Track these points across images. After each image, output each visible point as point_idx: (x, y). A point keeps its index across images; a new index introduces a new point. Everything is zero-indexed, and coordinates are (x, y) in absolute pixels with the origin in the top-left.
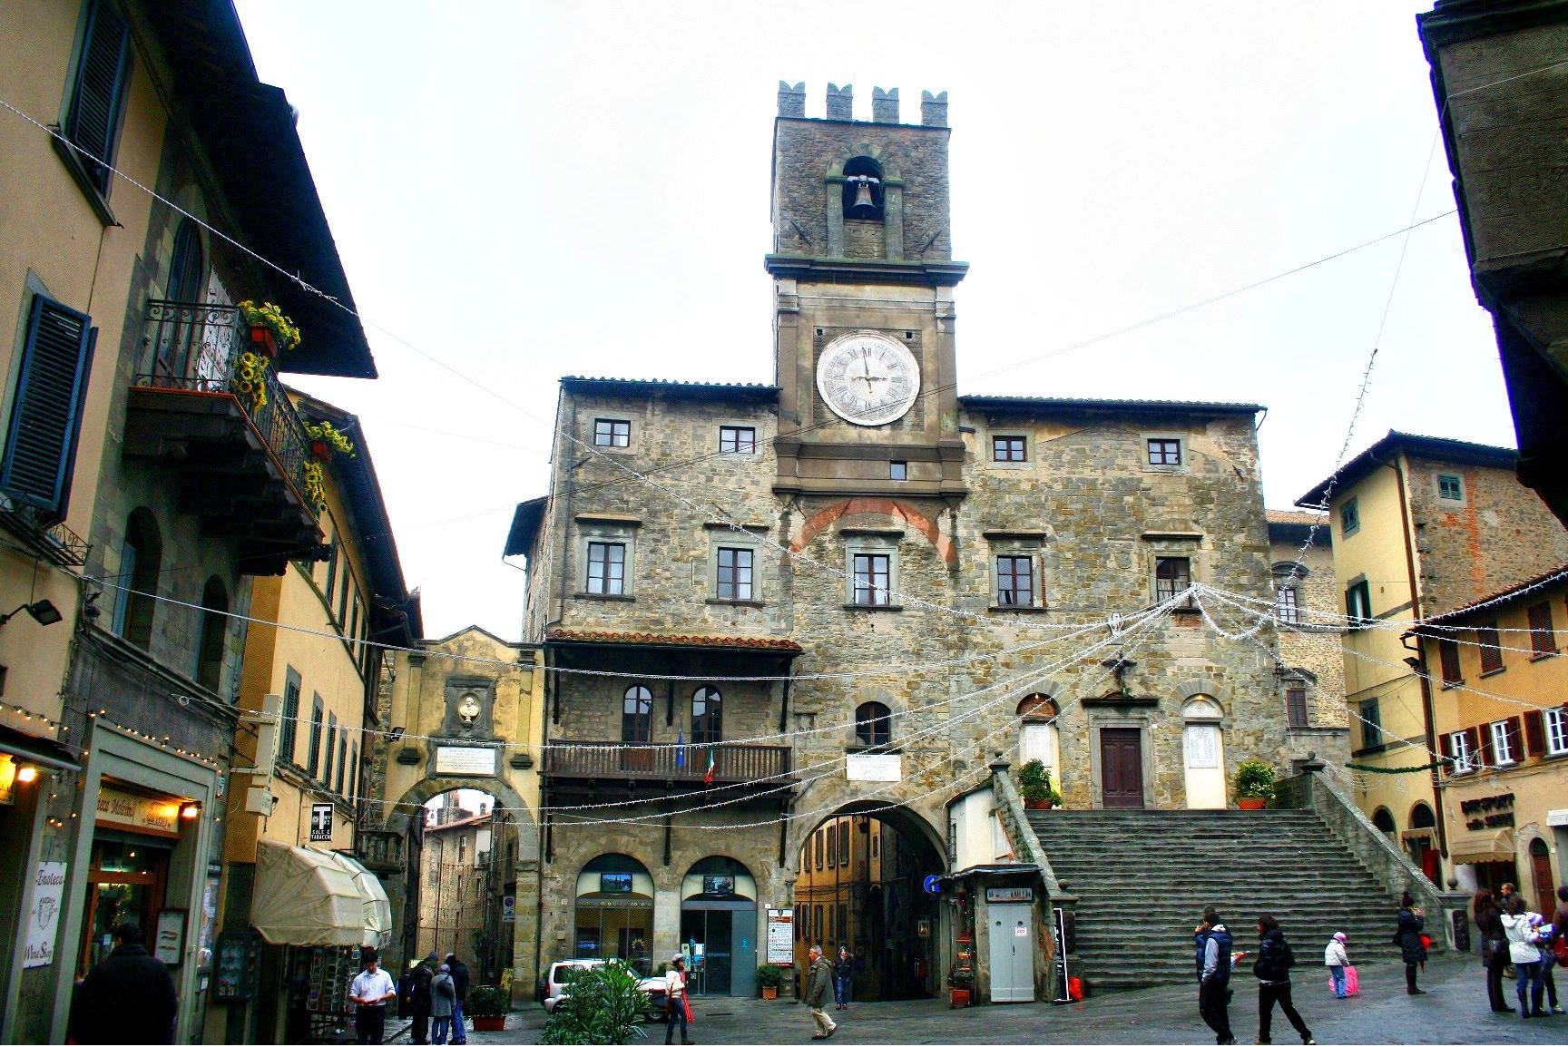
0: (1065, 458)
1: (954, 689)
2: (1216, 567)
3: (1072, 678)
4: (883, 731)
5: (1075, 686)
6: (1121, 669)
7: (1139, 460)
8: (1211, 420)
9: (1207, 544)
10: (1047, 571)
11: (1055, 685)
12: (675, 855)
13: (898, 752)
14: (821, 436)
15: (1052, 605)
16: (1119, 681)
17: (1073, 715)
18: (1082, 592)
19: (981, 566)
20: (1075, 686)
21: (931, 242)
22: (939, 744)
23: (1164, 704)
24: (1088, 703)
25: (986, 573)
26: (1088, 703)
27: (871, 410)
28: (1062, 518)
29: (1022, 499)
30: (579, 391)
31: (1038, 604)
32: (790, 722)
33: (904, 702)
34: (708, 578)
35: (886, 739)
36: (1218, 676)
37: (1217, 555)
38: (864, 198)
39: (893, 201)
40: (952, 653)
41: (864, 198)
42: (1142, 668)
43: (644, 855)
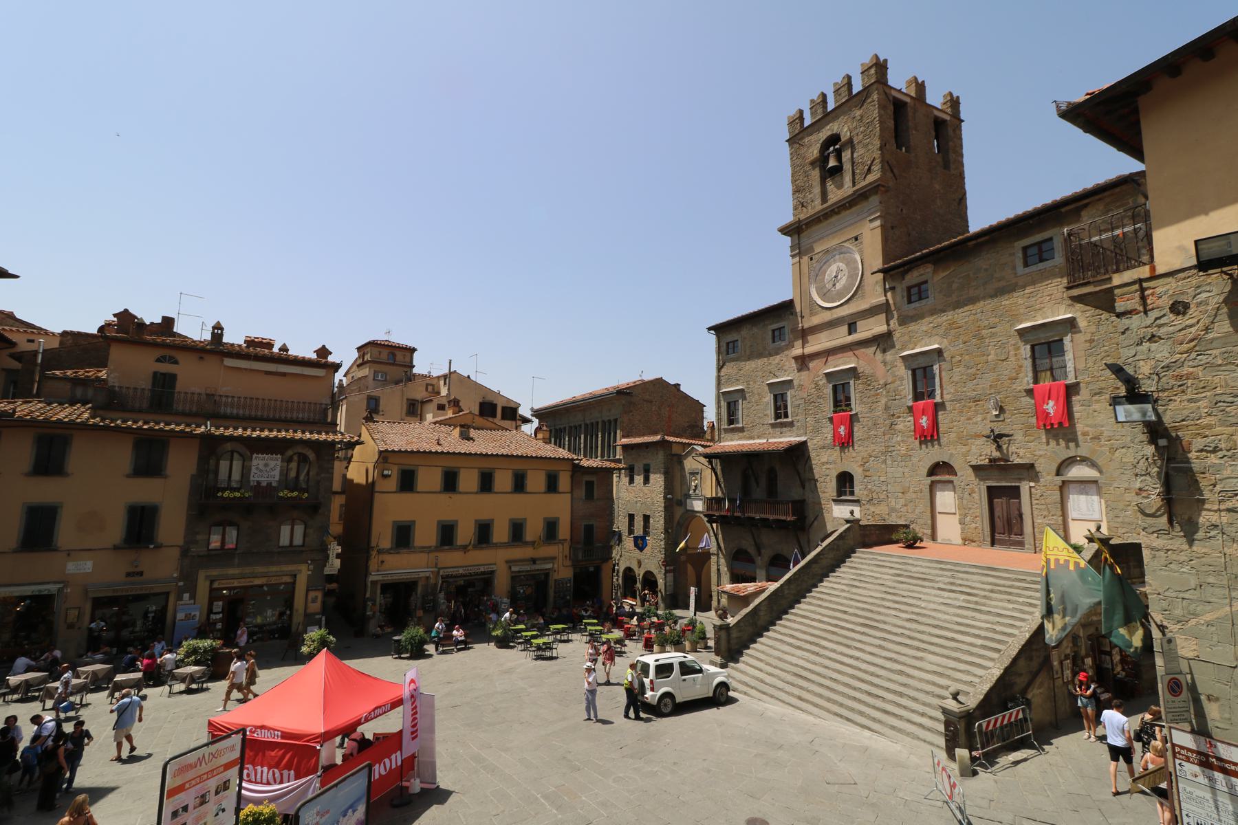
0: (955, 286)
1: (889, 462)
2: (1091, 341)
3: (965, 449)
4: (852, 486)
5: (965, 455)
6: (997, 438)
7: (1014, 268)
8: (1086, 206)
9: (1082, 323)
10: (943, 373)
11: (952, 455)
12: (763, 551)
13: (857, 501)
14: (816, 320)
15: (947, 397)
16: (999, 448)
17: (965, 475)
18: (970, 384)
19: (902, 379)
20: (965, 455)
21: (869, 169)
22: (882, 497)
23: (1039, 466)
24: (976, 468)
25: (905, 382)
26: (976, 468)
27: (840, 295)
28: (953, 332)
29: (925, 328)
30: (720, 329)
31: (938, 399)
32: (807, 485)
33: (860, 470)
34: (771, 411)
35: (852, 493)
36: (1096, 438)
37: (1093, 329)
38: (832, 163)
39: (846, 155)
40: (887, 437)
41: (832, 163)
42: (1019, 436)
43: (752, 550)
